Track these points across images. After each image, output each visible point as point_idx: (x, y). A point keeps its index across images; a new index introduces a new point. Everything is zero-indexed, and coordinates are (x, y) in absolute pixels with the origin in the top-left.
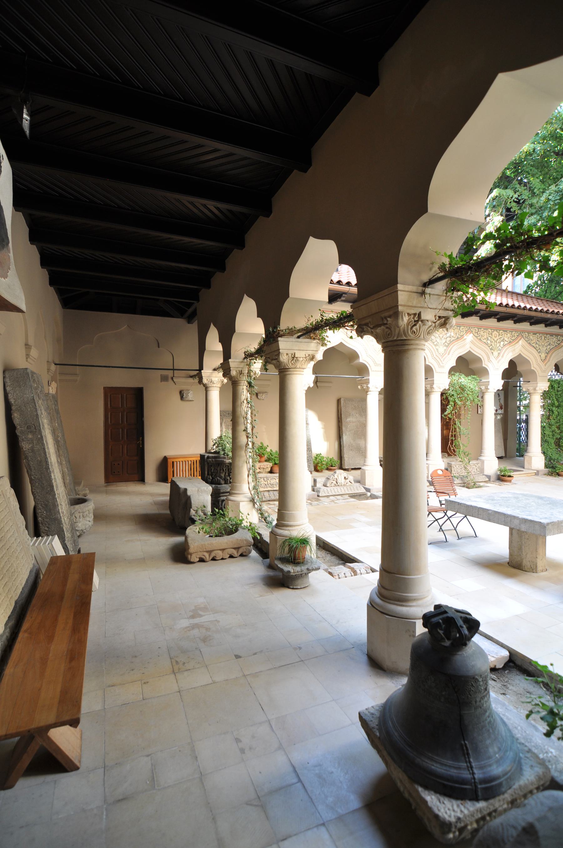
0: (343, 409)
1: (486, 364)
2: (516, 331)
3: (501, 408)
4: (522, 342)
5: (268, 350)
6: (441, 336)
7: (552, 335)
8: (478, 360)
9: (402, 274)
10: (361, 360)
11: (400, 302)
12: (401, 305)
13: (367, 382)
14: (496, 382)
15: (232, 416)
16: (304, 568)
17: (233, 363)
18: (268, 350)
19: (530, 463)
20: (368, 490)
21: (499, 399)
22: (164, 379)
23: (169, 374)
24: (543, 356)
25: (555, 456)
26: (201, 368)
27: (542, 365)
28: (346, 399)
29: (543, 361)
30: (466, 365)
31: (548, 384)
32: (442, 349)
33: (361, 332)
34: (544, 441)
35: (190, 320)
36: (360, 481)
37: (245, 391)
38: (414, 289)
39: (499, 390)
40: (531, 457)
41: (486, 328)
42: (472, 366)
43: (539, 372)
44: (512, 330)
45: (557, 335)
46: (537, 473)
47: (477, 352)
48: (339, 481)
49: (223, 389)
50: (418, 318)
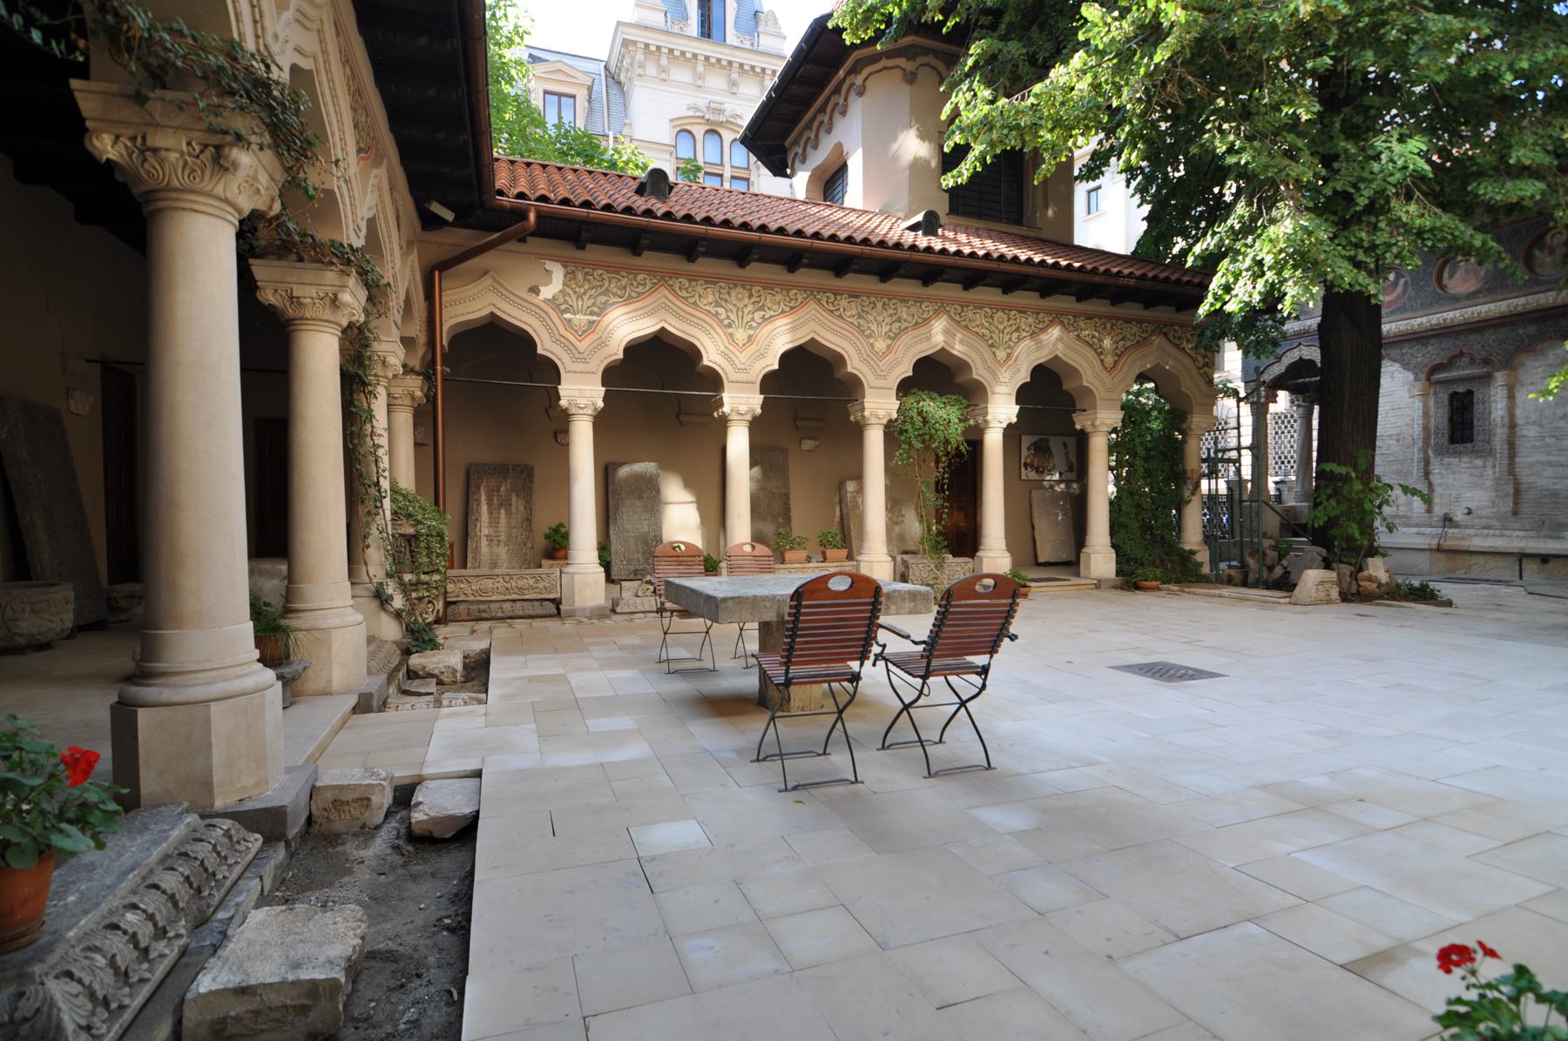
2: (1047, 312)
3: (1071, 469)
6: (880, 318)
7: (1128, 321)
11: (85, 114)
12: (93, 119)
19: (1088, 566)
21: (1067, 454)
24: (1109, 360)
29: (1109, 370)
31: (1121, 414)
32: (881, 345)
38: (115, 87)
39: (1010, 425)
40: (1088, 555)
43: (1099, 392)
46: (1099, 585)
47: (958, 350)
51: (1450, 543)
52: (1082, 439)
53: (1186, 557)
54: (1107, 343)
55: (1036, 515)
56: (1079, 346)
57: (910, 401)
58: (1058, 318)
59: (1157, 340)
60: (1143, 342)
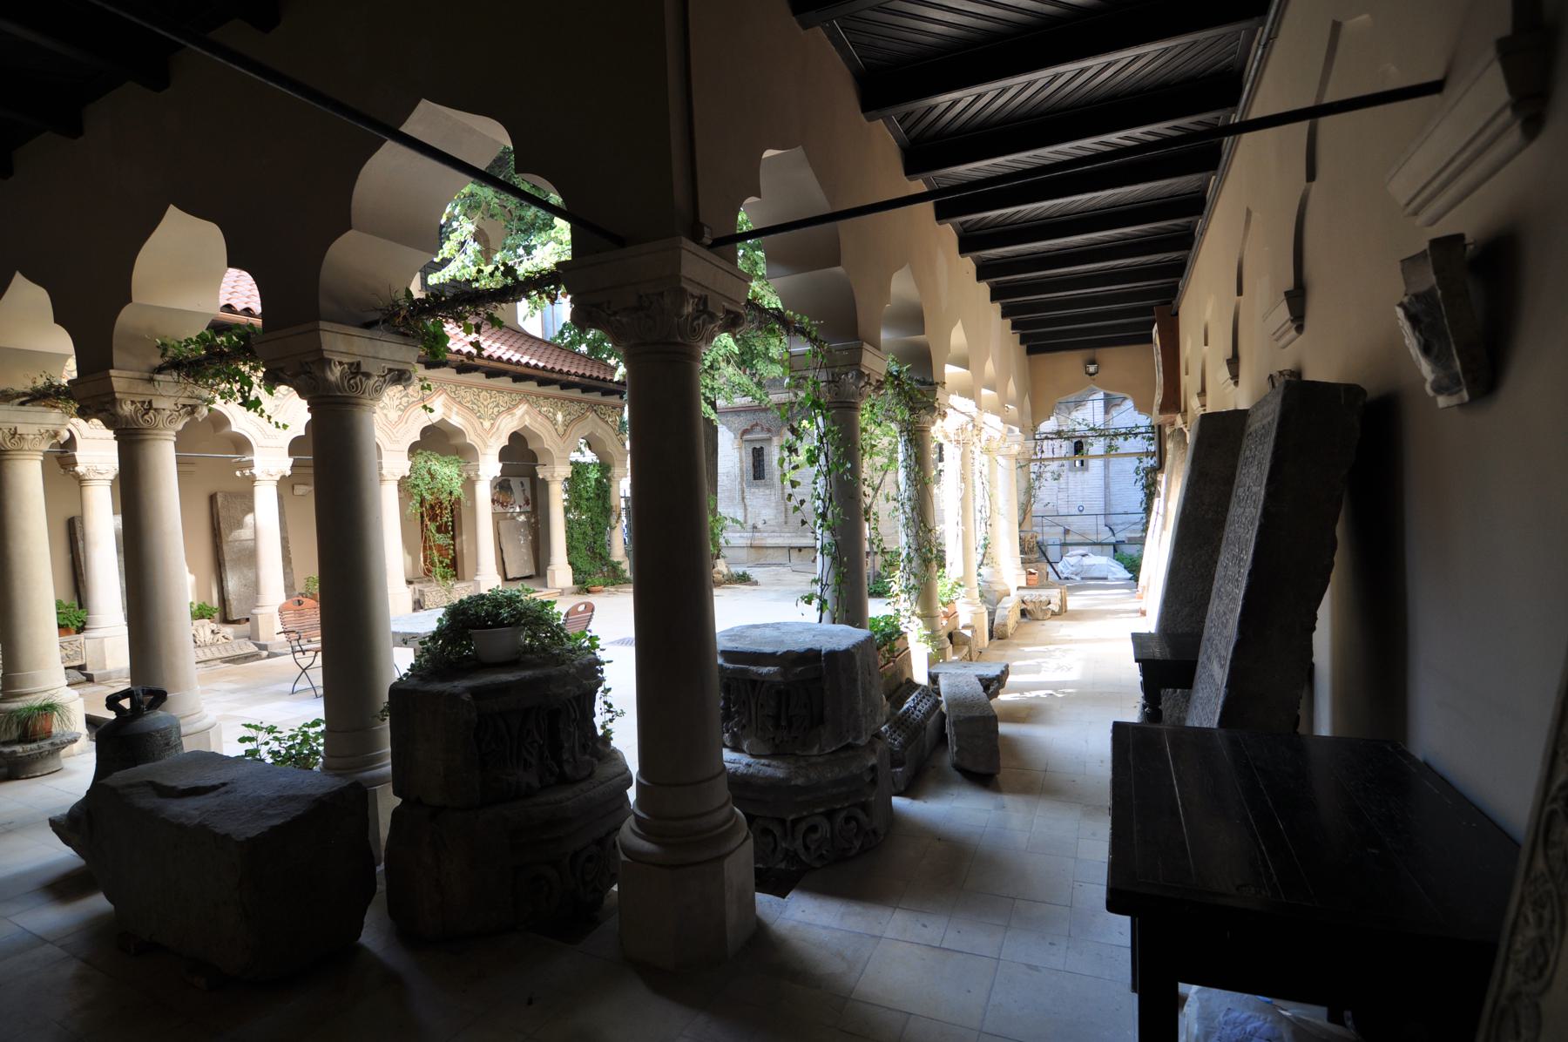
0: (222, 513)
1: (471, 438)
2: (518, 392)
4: (523, 408)
7: (572, 401)
8: (459, 432)
9: (117, 357)
10: (234, 428)
13: (250, 465)
14: (490, 467)
16: (45, 745)
20: (263, 647)
24: (561, 429)
25: (586, 567)
27: (558, 440)
28: (227, 495)
29: (561, 437)
30: (437, 440)
33: (84, 414)
34: (571, 549)
36: (253, 636)
41: (469, 386)
42: (455, 441)
43: (555, 452)
44: (511, 392)
45: (579, 401)
47: (456, 420)
48: (201, 638)
50: (149, 407)
51: (757, 543)
52: (545, 484)
53: (615, 567)
54: (560, 417)
55: (503, 540)
56: (539, 418)
57: (420, 460)
58: (525, 397)
59: (591, 415)
60: (581, 417)
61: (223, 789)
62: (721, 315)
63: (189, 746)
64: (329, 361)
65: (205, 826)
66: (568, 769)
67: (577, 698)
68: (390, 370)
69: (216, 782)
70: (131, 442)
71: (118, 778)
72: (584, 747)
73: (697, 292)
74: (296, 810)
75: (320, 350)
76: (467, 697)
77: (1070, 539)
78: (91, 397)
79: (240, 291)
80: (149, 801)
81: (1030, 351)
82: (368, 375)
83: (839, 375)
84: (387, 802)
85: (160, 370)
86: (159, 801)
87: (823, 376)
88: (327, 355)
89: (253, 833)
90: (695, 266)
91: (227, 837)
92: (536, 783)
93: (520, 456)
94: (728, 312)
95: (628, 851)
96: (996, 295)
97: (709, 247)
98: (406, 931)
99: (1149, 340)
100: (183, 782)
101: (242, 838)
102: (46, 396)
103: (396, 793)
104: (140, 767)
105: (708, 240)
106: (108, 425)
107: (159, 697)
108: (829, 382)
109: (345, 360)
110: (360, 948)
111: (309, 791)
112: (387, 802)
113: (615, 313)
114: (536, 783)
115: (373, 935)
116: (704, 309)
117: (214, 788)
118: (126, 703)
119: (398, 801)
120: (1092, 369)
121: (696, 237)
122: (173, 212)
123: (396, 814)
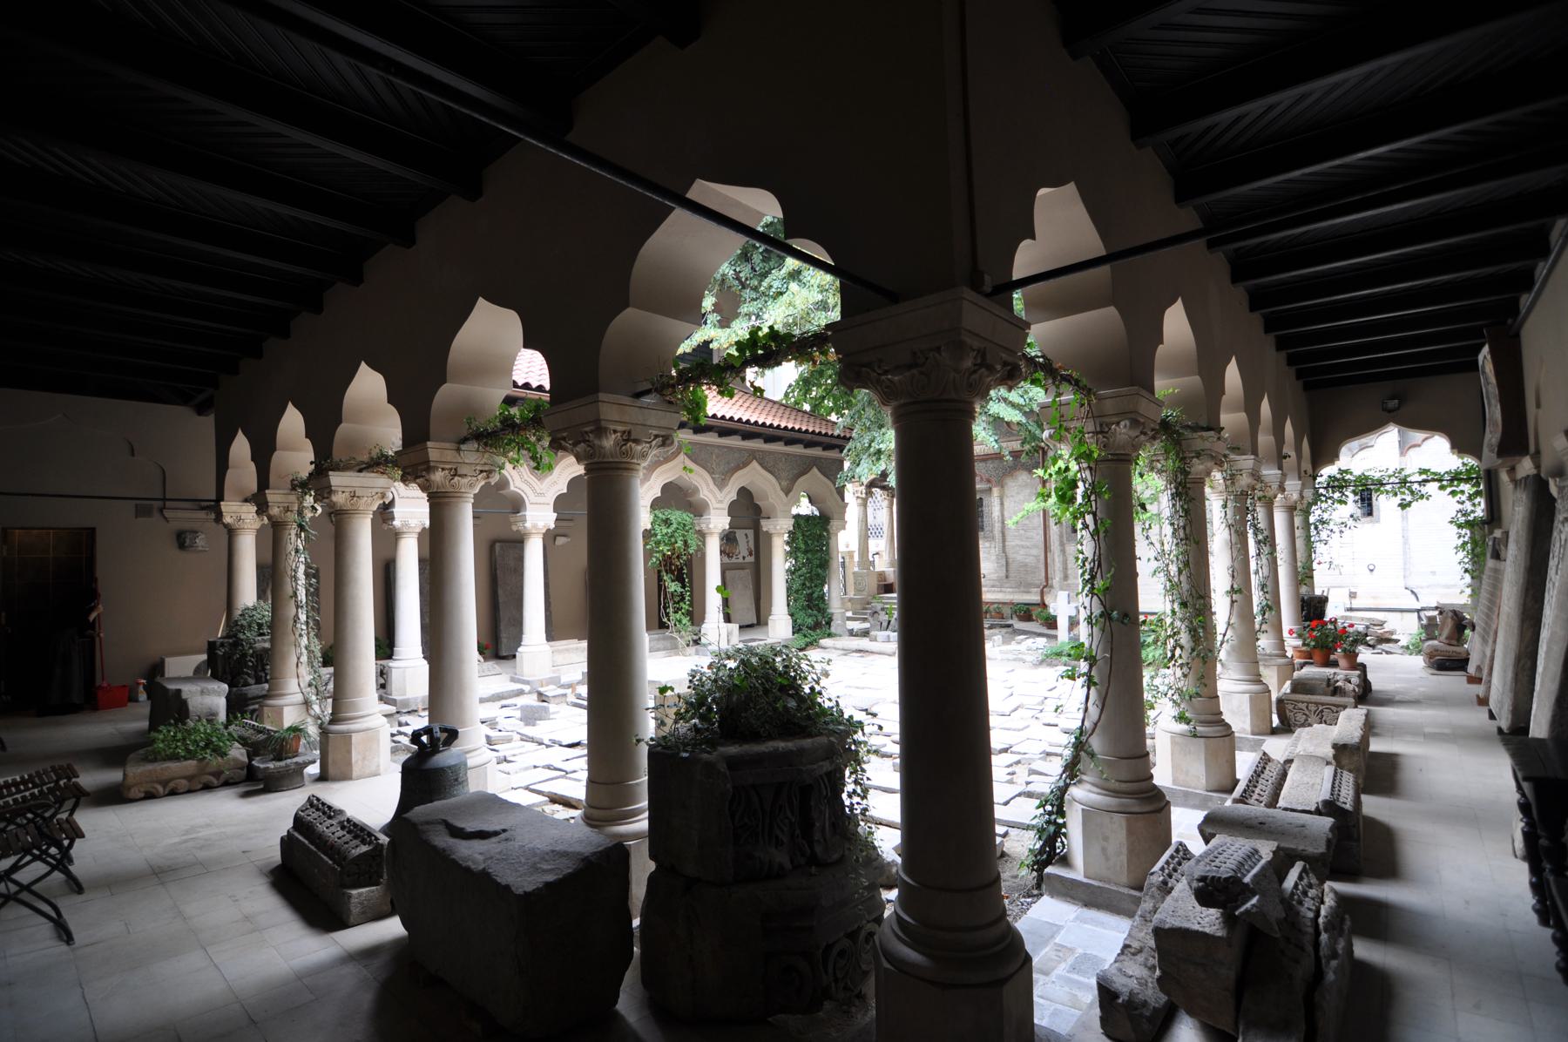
5: (317, 482)
14: (718, 521)
15: (270, 576)
17: (272, 496)
18: (317, 482)
22: (142, 512)
23: (152, 505)
26: (220, 497)
30: (675, 496)
35: (201, 410)
37: (293, 537)
49: (260, 534)
52: (769, 536)
61: (503, 836)
62: (998, 367)
63: (474, 785)
64: (606, 429)
65: (488, 875)
66: (818, 849)
67: (828, 774)
68: (656, 436)
69: (498, 828)
70: (440, 504)
71: (419, 812)
72: (833, 825)
73: (976, 344)
74: (567, 867)
75: (598, 421)
76: (723, 767)
77: (1356, 604)
78: (412, 465)
79: (532, 368)
80: (442, 840)
81: (1307, 387)
82: (637, 441)
83: (1109, 425)
84: (642, 868)
85: (464, 441)
86: (452, 841)
87: (1090, 426)
88: (603, 424)
89: (529, 888)
90: (974, 314)
91: (507, 887)
92: (788, 865)
93: (748, 511)
94: (1005, 364)
95: (890, 957)
96: (1269, 326)
97: (988, 295)
98: (658, 1006)
99: (1474, 366)
100: (471, 826)
101: (520, 891)
102: (378, 463)
103: (652, 857)
104: (437, 804)
105: (988, 289)
106: (423, 488)
107: (453, 735)
108: (1096, 433)
109: (620, 428)
110: (617, 1016)
111: (578, 848)
112: (642, 868)
113: (886, 372)
114: (788, 865)
115: (628, 1004)
116: (984, 363)
117: (496, 834)
118: (424, 739)
119: (652, 866)
120: (1393, 404)
121: (976, 285)
122: (481, 299)
123: (652, 879)
